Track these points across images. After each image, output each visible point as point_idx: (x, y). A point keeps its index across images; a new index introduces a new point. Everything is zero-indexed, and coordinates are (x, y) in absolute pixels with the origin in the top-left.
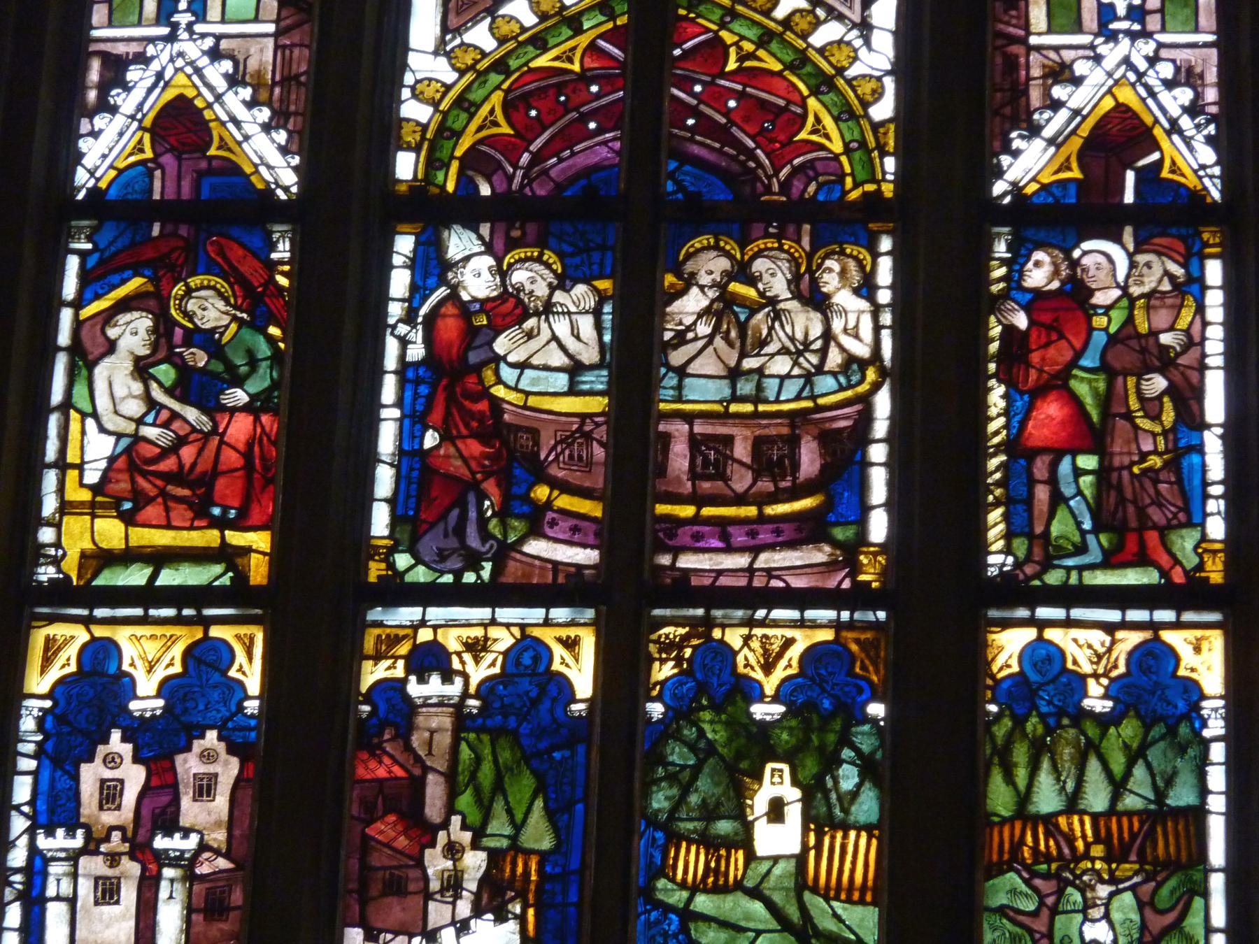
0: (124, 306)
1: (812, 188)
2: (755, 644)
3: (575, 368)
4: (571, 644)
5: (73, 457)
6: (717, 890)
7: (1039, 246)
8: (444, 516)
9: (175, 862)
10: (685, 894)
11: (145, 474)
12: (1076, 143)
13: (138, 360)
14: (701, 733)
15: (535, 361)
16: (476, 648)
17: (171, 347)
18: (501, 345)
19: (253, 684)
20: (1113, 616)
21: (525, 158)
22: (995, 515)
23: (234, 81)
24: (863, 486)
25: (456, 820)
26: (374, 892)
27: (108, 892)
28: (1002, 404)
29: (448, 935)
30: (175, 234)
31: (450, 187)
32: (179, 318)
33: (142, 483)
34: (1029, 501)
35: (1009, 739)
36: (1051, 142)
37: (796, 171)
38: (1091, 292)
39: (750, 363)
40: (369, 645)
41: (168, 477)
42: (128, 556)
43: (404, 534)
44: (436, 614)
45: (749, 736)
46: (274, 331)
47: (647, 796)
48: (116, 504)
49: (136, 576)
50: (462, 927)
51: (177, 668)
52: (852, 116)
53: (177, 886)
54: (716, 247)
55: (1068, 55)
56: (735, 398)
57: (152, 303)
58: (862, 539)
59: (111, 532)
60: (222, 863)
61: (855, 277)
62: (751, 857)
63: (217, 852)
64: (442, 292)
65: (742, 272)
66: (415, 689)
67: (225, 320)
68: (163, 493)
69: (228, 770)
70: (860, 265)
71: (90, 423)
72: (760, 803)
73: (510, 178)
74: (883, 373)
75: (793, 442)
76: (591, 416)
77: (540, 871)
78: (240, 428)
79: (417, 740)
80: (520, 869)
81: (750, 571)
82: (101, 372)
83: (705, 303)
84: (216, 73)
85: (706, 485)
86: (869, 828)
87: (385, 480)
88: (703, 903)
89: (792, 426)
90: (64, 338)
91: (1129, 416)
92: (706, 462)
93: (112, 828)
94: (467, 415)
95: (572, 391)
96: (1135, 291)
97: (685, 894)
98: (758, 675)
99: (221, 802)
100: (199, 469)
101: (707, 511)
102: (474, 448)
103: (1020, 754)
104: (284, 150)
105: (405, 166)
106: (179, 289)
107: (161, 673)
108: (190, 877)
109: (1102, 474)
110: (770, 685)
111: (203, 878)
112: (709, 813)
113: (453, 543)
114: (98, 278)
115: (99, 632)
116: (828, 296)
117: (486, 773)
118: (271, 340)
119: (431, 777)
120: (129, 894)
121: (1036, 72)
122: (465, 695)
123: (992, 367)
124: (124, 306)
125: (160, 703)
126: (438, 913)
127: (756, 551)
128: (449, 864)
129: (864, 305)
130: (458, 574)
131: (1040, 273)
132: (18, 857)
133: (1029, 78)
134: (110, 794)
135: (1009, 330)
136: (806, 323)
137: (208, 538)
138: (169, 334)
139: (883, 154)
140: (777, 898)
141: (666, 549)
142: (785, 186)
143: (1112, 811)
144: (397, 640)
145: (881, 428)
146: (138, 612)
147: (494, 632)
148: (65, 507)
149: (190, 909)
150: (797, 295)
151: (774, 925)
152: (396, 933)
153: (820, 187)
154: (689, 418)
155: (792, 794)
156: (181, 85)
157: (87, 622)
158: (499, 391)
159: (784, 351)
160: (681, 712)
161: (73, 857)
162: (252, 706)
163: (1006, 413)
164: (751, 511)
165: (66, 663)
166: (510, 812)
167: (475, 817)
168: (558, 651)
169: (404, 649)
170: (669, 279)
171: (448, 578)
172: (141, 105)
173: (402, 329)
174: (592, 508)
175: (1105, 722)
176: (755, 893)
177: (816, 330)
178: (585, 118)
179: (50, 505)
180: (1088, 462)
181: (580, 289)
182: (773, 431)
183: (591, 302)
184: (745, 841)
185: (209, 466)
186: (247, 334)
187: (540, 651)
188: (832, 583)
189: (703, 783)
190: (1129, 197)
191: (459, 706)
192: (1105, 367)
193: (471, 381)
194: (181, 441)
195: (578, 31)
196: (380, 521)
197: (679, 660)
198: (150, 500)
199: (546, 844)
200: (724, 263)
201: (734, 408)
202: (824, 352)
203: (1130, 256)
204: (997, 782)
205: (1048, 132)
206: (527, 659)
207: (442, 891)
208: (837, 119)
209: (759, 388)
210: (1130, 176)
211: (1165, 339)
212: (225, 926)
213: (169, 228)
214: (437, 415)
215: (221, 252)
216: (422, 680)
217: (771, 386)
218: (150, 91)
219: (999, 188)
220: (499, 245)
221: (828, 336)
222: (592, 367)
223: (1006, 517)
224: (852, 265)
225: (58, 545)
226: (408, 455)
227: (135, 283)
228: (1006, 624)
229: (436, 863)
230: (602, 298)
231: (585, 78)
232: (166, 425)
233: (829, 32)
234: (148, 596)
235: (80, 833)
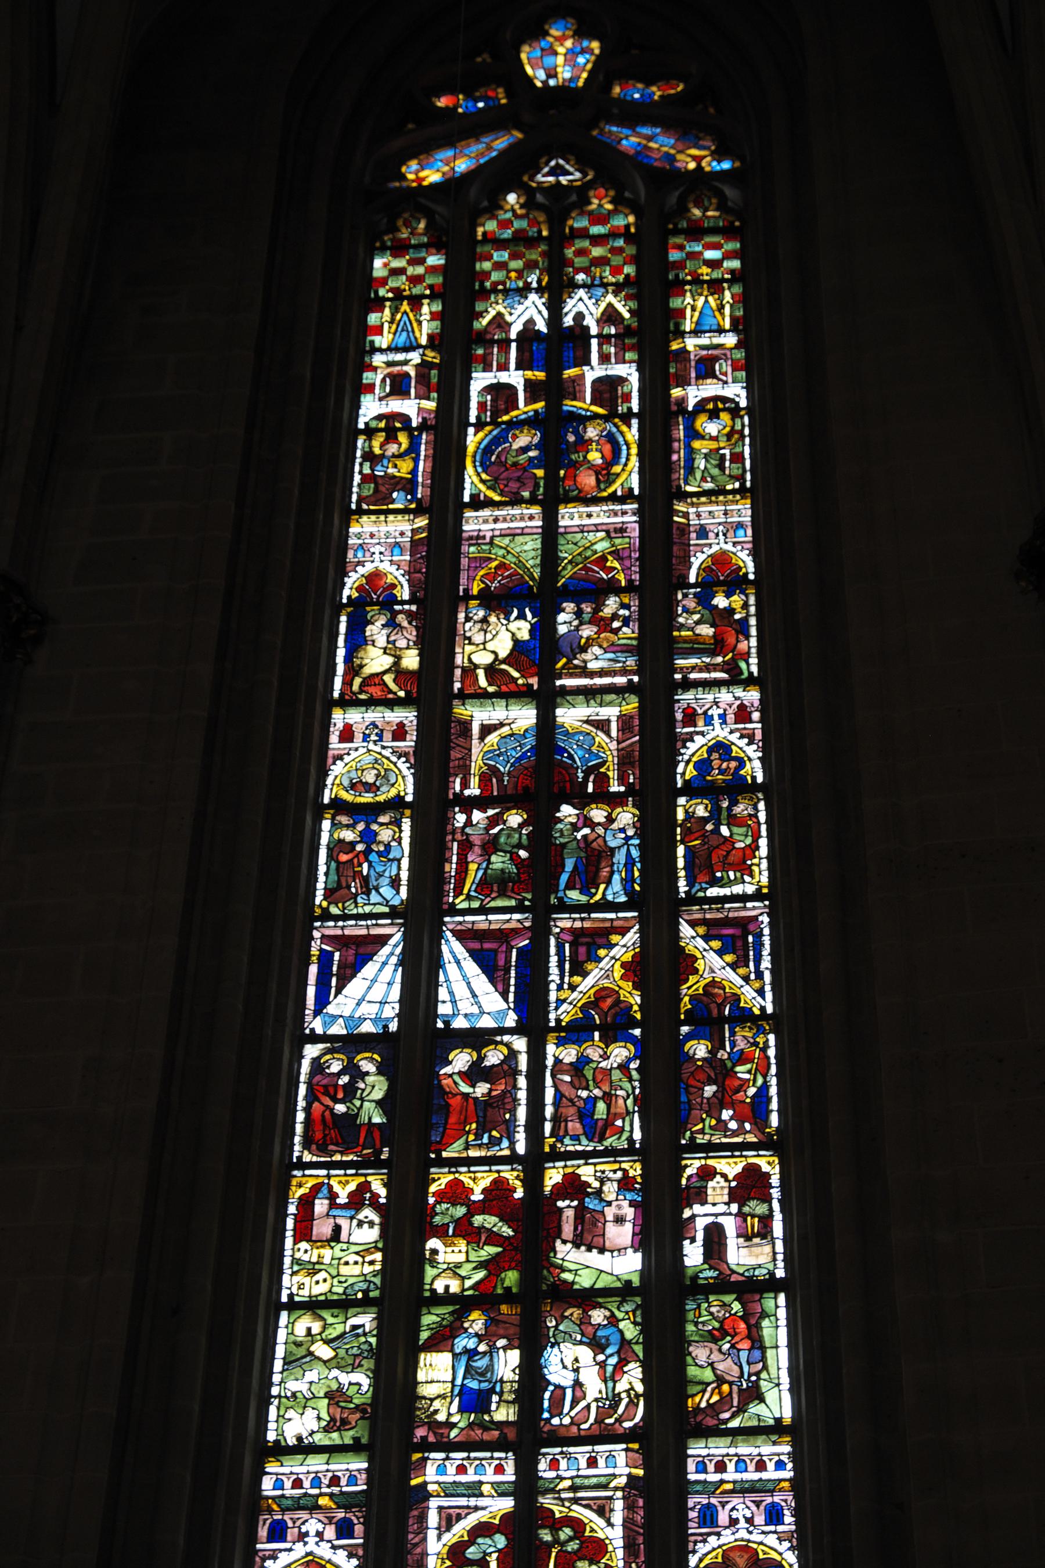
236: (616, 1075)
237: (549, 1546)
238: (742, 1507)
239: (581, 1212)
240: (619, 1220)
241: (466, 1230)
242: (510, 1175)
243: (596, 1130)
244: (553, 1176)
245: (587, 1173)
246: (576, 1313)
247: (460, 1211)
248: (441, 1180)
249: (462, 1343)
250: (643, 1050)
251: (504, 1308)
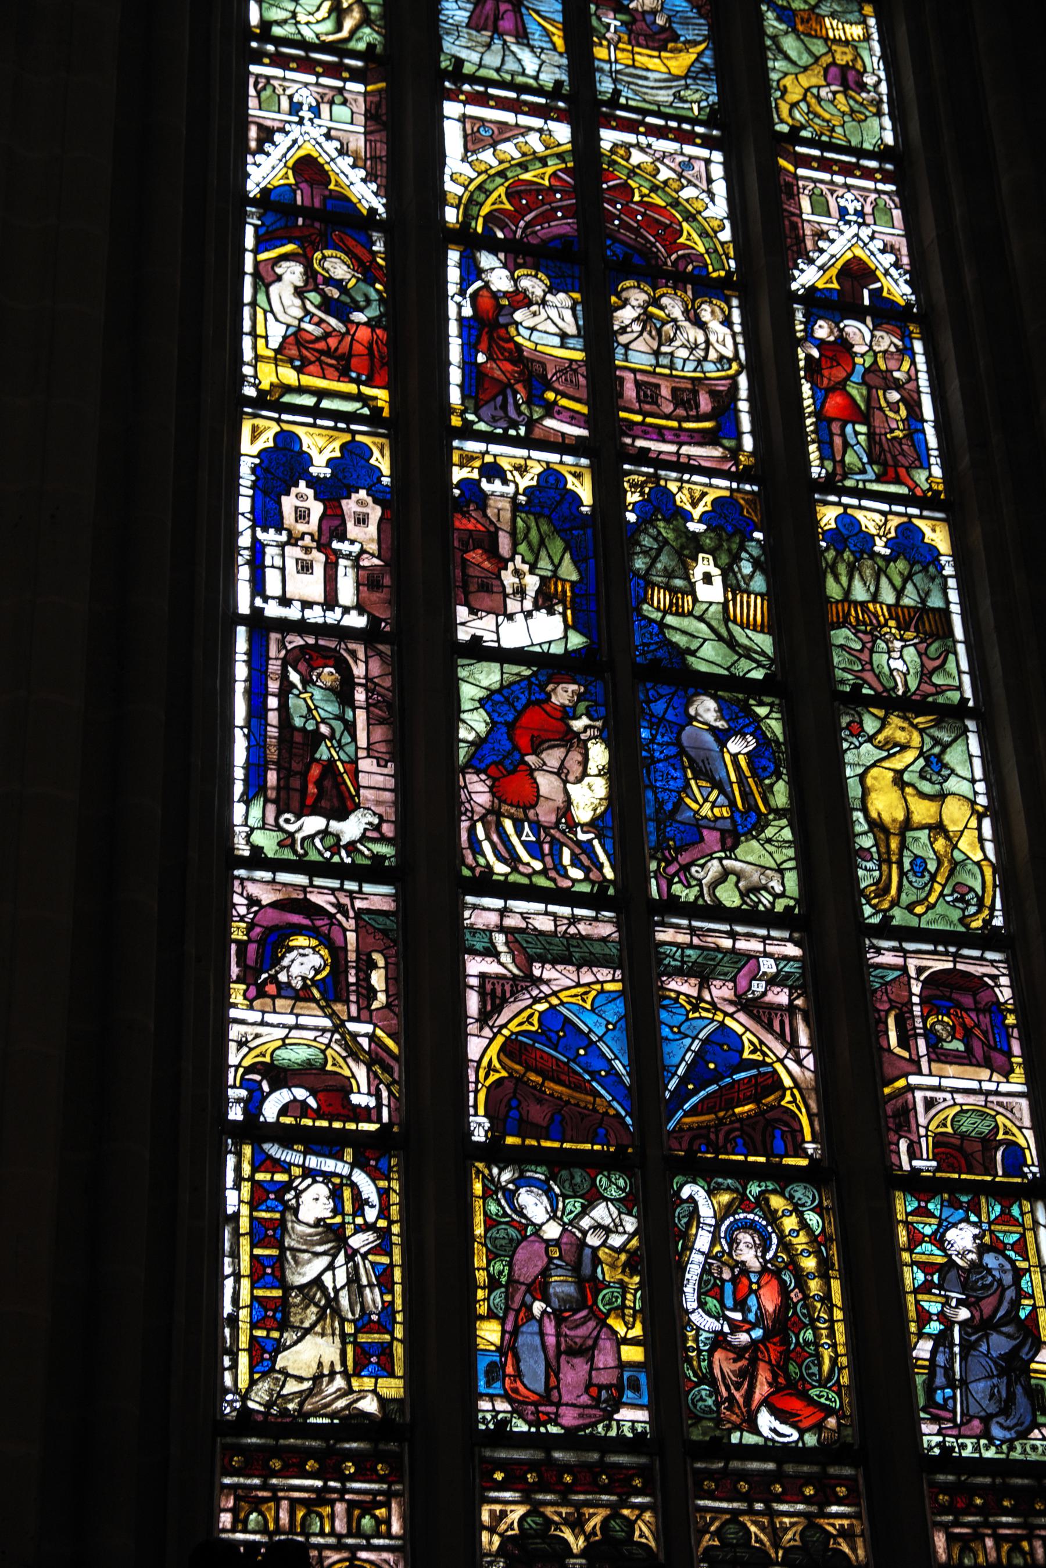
0: (285, 257)
1: (690, 268)
2: (685, 491)
3: (563, 336)
4: (577, 476)
5: (260, 331)
6: (677, 614)
7: (821, 318)
8: (494, 398)
9: (348, 556)
10: (660, 615)
11: (307, 348)
12: (833, 272)
13: (296, 288)
14: (660, 533)
15: (539, 327)
16: (522, 470)
17: (317, 285)
18: (518, 316)
19: (385, 467)
20: (885, 507)
21: (522, 224)
22: (813, 448)
23: (342, 152)
24: (737, 422)
25: (518, 558)
26: (473, 588)
27: (306, 567)
28: (810, 393)
29: (520, 617)
30: (312, 226)
31: (480, 230)
32: (320, 270)
33: (305, 353)
34: (831, 443)
35: (835, 560)
36: (820, 268)
37: (679, 257)
38: (853, 346)
39: (664, 349)
40: (456, 459)
41: (322, 352)
42: (301, 390)
43: (470, 404)
44: (494, 449)
45: (687, 538)
46: (378, 286)
47: (632, 560)
48: (291, 361)
49: (309, 401)
50: (528, 615)
51: (338, 454)
52: (708, 235)
53: (350, 571)
54: (639, 287)
55: (825, 228)
56: (658, 365)
57: (302, 259)
58: (739, 447)
59: (289, 376)
60: (376, 561)
61: (721, 317)
62: (695, 600)
63: (373, 555)
64: (479, 284)
65: (655, 302)
66: (485, 485)
67: (348, 276)
68: (318, 360)
69: (375, 513)
70: (722, 310)
71: (269, 316)
72: (697, 573)
73: (515, 232)
74: (740, 364)
75: (695, 393)
76: (576, 361)
77: (572, 591)
78: (364, 334)
79: (490, 512)
80: (560, 589)
81: (678, 454)
82: (274, 290)
83: (636, 315)
84: (331, 147)
85: (647, 407)
86: (762, 595)
87: (455, 375)
88: (670, 620)
89: (693, 384)
90: (249, 267)
91: (881, 409)
92: (645, 394)
93: (304, 534)
94: (502, 350)
95: (563, 346)
96: (876, 348)
97: (660, 615)
98: (688, 507)
99: (372, 529)
100: (340, 351)
101: (649, 420)
102: (508, 367)
103: (842, 569)
104: (376, 194)
105: (451, 215)
106: (318, 255)
107: (327, 455)
108: (357, 566)
109: (870, 435)
110: (697, 513)
111: (364, 568)
112: (669, 574)
113: (501, 413)
114: (267, 241)
115: (286, 427)
116: (705, 323)
117: (534, 535)
118: (377, 290)
119: (501, 533)
120: (319, 569)
121: (808, 232)
122: (517, 493)
123: (802, 373)
124: (285, 257)
125: (328, 471)
126: (512, 605)
127: (681, 445)
128: (517, 580)
129: (727, 331)
130: (506, 430)
131: (822, 330)
132: (245, 541)
133: (804, 235)
134: (302, 515)
135: (809, 357)
136: (695, 334)
137: (352, 388)
138: (315, 279)
139: (728, 258)
140: (714, 623)
141: (629, 436)
142: (675, 263)
143: (897, 604)
144: (473, 459)
145: (743, 393)
146: (310, 420)
147: (529, 463)
148: (257, 358)
149: (358, 584)
150: (688, 319)
151: (713, 637)
152: (488, 613)
153: (694, 268)
154: (634, 371)
155: (715, 572)
156: (308, 149)
157: (278, 421)
158: (518, 339)
159: (683, 346)
160: (647, 518)
161: (282, 546)
162: (386, 481)
163: (813, 397)
164: (675, 424)
165: (267, 440)
166: (550, 557)
167: (530, 557)
168: (570, 479)
169: (477, 464)
170: (613, 299)
171: (500, 431)
172: (284, 155)
173: (458, 298)
174: (584, 409)
175: (888, 559)
176: (701, 619)
177: (701, 339)
178: (555, 210)
179: (248, 355)
180: (862, 428)
181: (562, 296)
182: (683, 386)
183: (569, 303)
184: (693, 593)
185: (347, 350)
186: (362, 285)
187: (561, 479)
188: (726, 467)
189: (663, 558)
190: (867, 302)
191: (514, 499)
192: (864, 382)
193: (502, 332)
194: (327, 335)
195: (545, 165)
196: (455, 397)
197: (642, 494)
198: (311, 363)
199: (575, 577)
200: (644, 297)
201: (658, 370)
202: (707, 350)
203: (871, 332)
204: (830, 581)
205: (819, 263)
206: (552, 480)
207: (514, 594)
208: (700, 236)
209: (672, 362)
210: (866, 293)
211: (896, 374)
212: (382, 595)
213: (308, 222)
214: (484, 345)
215: (342, 241)
216: (489, 481)
217: (679, 364)
218: (289, 149)
219: (794, 286)
220: (511, 265)
221: (707, 342)
222: (573, 336)
223: (819, 449)
224: (717, 310)
225: (255, 377)
226: (468, 365)
227: (290, 248)
228: (826, 503)
229: (508, 579)
230: (575, 303)
231: (552, 190)
232: (318, 324)
233: (688, 193)
234: (315, 412)
235: (284, 533)
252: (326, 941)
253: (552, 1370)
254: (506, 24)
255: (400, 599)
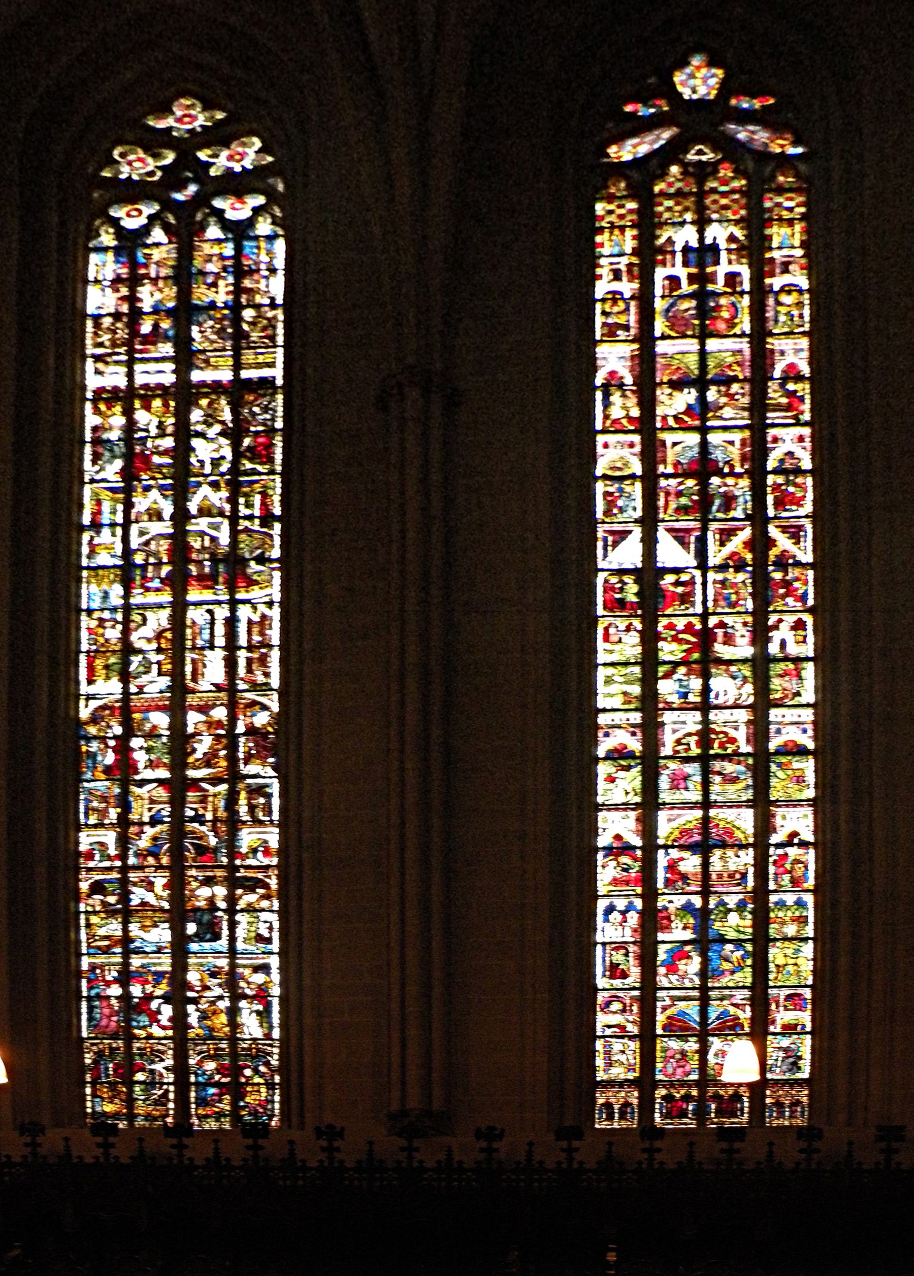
236: (740, 585)
237: (715, 739)
238: (793, 728)
239: (726, 634)
240: (743, 636)
241: (675, 639)
242: (695, 620)
243: (733, 605)
244: (712, 621)
245: (728, 620)
246: (724, 667)
247: (673, 633)
248: (664, 622)
249: (675, 677)
250: (754, 575)
251: (694, 666)
252: (622, 1002)
253: (675, 1070)
254: (682, 786)
255: (643, 934)
